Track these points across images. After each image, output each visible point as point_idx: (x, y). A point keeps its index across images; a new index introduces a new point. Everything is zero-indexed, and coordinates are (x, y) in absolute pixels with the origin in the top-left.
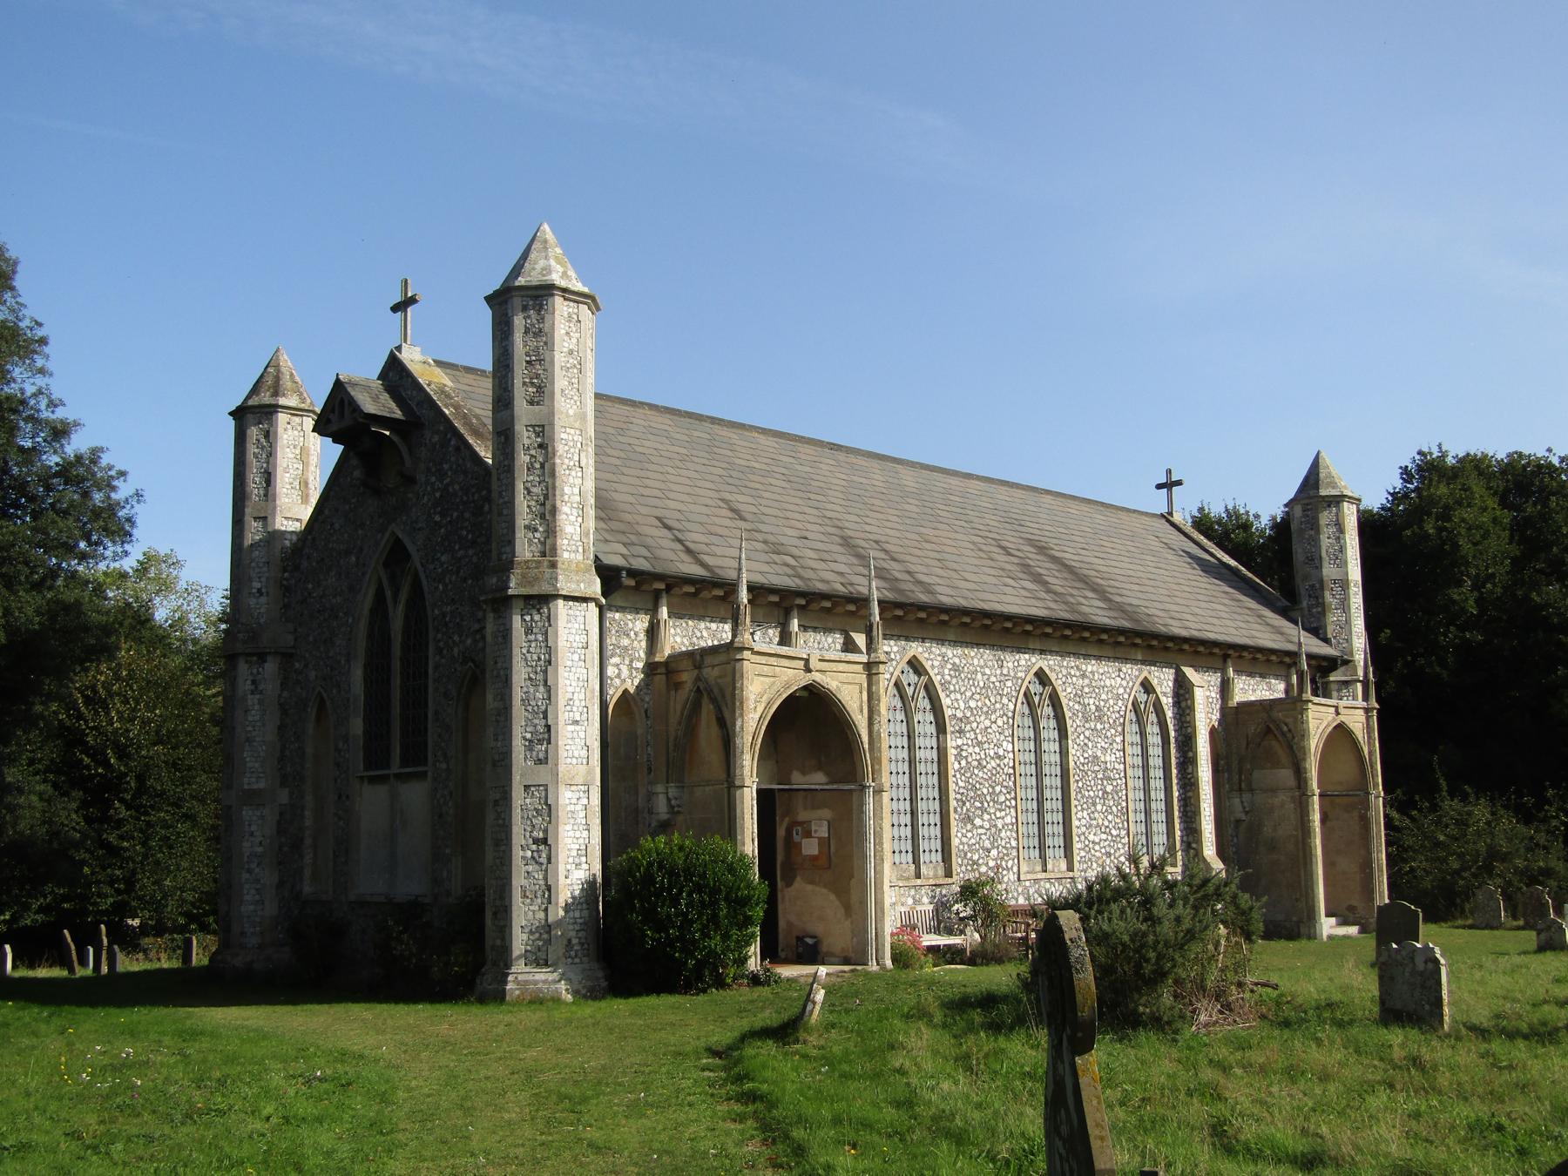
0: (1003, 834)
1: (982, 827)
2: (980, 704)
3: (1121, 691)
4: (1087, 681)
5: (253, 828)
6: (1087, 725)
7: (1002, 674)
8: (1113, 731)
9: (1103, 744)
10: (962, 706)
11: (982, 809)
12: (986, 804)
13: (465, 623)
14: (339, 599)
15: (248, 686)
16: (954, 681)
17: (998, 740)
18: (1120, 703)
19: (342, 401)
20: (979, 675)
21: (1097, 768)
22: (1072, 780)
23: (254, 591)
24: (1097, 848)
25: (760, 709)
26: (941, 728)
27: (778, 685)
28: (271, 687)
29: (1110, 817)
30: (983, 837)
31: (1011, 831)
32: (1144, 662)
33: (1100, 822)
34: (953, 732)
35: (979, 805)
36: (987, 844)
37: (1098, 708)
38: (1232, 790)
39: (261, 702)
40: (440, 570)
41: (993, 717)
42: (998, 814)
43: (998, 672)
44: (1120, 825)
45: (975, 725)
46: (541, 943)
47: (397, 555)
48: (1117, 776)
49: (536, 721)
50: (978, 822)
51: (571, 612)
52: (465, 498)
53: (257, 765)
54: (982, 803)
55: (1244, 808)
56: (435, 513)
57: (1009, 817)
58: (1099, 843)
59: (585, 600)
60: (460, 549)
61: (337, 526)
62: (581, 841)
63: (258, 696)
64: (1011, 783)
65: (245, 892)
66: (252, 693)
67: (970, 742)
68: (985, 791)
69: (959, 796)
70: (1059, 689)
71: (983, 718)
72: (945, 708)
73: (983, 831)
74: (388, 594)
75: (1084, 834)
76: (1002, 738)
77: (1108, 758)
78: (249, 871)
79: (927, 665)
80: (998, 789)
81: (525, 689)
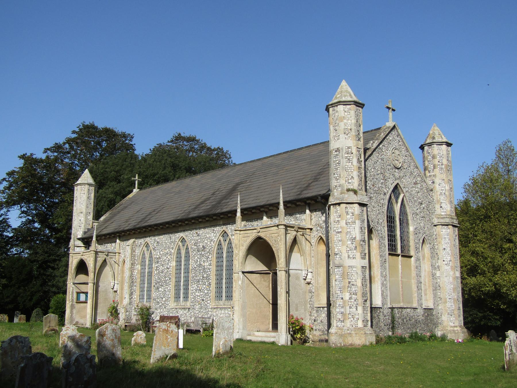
1: (161, 291)
6: (198, 253)
9: (204, 259)
18: (212, 243)
21: (201, 268)
29: (204, 286)
30: (161, 294)
32: (224, 224)
36: (162, 296)
37: (203, 247)
43: (170, 241)
45: (161, 259)
58: (199, 296)
69: (155, 282)
73: (161, 292)
77: (205, 264)
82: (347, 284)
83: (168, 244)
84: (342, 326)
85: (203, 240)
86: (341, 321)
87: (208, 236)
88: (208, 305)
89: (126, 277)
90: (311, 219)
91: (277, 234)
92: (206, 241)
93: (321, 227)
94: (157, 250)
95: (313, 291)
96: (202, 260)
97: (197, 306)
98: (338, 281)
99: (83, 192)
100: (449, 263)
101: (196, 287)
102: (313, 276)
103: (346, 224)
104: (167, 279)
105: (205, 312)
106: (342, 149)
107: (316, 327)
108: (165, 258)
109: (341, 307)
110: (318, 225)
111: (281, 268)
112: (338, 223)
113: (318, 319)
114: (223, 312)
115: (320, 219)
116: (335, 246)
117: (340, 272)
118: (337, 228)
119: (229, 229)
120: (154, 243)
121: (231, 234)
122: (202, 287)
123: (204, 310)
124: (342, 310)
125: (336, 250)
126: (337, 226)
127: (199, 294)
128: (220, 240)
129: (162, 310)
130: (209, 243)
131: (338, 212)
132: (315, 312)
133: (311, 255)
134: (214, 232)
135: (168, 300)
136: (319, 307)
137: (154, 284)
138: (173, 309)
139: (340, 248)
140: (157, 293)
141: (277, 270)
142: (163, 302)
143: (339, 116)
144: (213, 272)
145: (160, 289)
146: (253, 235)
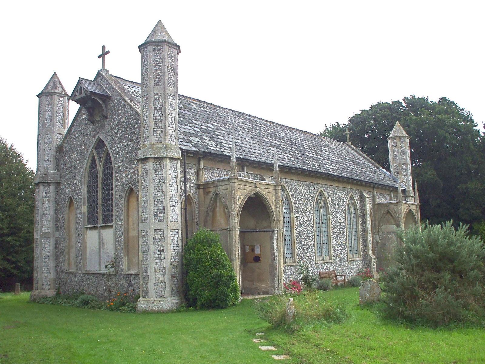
0: (310, 248)
1: (304, 245)
2: (303, 202)
3: (344, 199)
4: (334, 195)
5: (46, 246)
6: (335, 210)
7: (310, 192)
8: (342, 212)
11: (305, 239)
12: (305, 237)
13: (128, 169)
14: (78, 162)
15: (44, 194)
16: (295, 194)
17: (309, 215)
19: (81, 88)
20: (303, 192)
21: (338, 225)
22: (331, 229)
23: (46, 160)
24: (338, 252)
25: (240, 201)
26: (291, 210)
27: (246, 192)
28: (52, 195)
29: (342, 241)
30: (305, 249)
31: (313, 246)
33: (339, 243)
34: (295, 212)
35: (303, 237)
38: (376, 232)
39: (48, 200)
40: (117, 150)
41: (307, 207)
42: (309, 241)
43: (309, 191)
44: (345, 244)
45: (302, 209)
46: (162, 289)
47: (100, 144)
48: (344, 227)
49: (159, 205)
50: (303, 243)
51: (171, 164)
52: (127, 123)
53: (47, 223)
54: (304, 237)
55: (380, 238)
56: (115, 129)
57: (312, 242)
58: (339, 250)
59: (176, 159)
60: (125, 142)
61: (77, 136)
62: (176, 250)
63: (47, 198)
64: (313, 230)
65: (44, 269)
66: (45, 197)
67: (300, 216)
68: (305, 233)
70: (327, 197)
71: (304, 207)
72: (292, 203)
74: (97, 159)
75: (334, 247)
76: (310, 214)
77: (341, 221)
78: (45, 262)
79: (287, 188)
80: (309, 232)
81: (154, 193)
83: (307, 194)
135: (312, 255)
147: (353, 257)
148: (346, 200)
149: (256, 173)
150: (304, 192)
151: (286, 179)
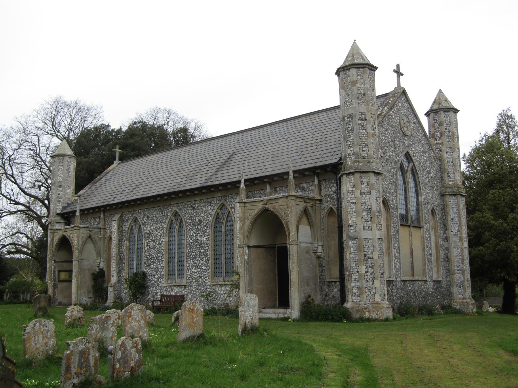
0: (160, 270)
1: (153, 268)
6: (194, 228)
9: (201, 234)
10: (149, 229)
11: (154, 262)
18: (209, 216)
20: (155, 218)
24: (196, 274)
29: (202, 262)
30: (153, 271)
36: (154, 273)
37: (199, 220)
42: (159, 263)
43: (161, 215)
45: (152, 235)
58: (196, 273)
69: (146, 258)
73: (153, 269)
77: (202, 239)
82: (363, 258)
84: (358, 301)
85: (199, 213)
86: (357, 295)
87: (204, 209)
88: (207, 282)
89: (114, 254)
90: (321, 190)
91: (287, 206)
92: (202, 215)
93: (332, 198)
94: (147, 225)
95: (324, 265)
96: (199, 235)
97: (193, 283)
98: (353, 254)
99: (61, 164)
100: (457, 233)
101: (193, 263)
102: (323, 249)
103: (361, 194)
104: (159, 255)
105: (203, 289)
106: (355, 115)
107: (327, 302)
108: (157, 233)
109: (356, 281)
110: (329, 196)
111: (292, 241)
112: (351, 194)
113: (330, 294)
114: (223, 288)
115: (330, 190)
116: (349, 217)
117: (355, 245)
118: (351, 199)
119: (228, 201)
120: (144, 217)
121: (230, 206)
122: (199, 263)
123: (201, 287)
124: (358, 284)
125: (350, 222)
126: (351, 196)
127: (196, 271)
128: (218, 213)
129: (154, 288)
130: (206, 217)
131: (352, 181)
132: (326, 286)
133: (321, 228)
134: (212, 205)
135: (161, 277)
136: (330, 282)
137: (145, 261)
138: (167, 287)
139: (354, 219)
140: (149, 271)
141: (287, 243)
142: (155, 280)
143: (352, 80)
144: (212, 247)
145: (152, 266)
146: (260, 208)
147: (224, 281)
148: (212, 213)
149: (114, 213)
150: (156, 217)
151: (138, 210)
